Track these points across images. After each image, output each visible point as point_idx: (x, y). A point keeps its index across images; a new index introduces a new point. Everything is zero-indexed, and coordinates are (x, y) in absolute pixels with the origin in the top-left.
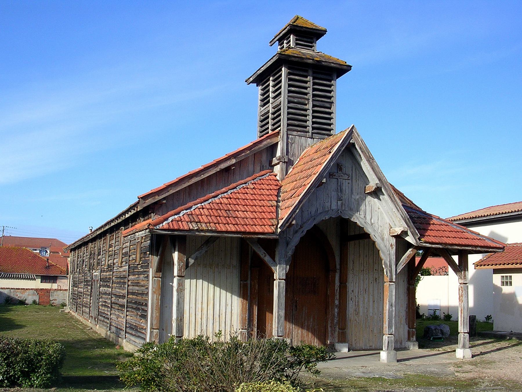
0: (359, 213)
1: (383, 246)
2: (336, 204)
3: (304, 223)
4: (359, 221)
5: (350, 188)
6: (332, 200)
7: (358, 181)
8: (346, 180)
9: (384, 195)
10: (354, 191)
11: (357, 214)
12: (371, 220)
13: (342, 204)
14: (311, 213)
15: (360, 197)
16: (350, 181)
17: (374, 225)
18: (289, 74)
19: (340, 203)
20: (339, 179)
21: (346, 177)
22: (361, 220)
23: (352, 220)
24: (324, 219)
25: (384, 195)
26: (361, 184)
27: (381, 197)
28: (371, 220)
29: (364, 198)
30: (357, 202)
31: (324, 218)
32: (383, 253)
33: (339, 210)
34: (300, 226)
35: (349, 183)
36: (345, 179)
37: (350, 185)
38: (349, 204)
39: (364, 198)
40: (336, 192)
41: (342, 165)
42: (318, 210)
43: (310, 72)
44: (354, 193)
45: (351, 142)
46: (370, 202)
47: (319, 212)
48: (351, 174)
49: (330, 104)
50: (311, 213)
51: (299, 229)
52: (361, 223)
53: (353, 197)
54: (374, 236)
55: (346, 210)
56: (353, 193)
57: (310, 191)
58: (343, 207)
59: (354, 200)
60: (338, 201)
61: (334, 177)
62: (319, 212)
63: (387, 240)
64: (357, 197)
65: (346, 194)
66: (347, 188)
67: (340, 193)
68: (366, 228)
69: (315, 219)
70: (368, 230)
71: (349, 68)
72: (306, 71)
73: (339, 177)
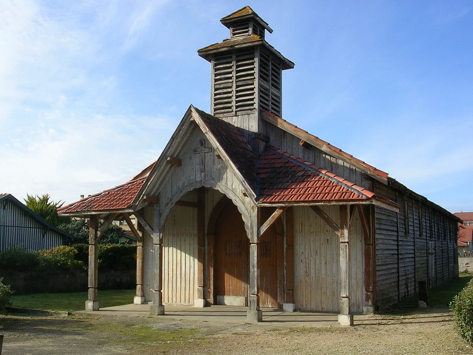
4: (220, 188)
8: (209, 153)
13: (205, 175)
17: (235, 190)
19: (203, 174)
20: (201, 154)
22: (222, 187)
24: (189, 190)
28: (232, 186)
30: (219, 171)
32: (245, 216)
33: (202, 181)
34: (170, 199)
35: (211, 155)
42: (184, 184)
43: (234, 57)
44: (216, 163)
47: (185, 185)
52: (222, 190)
53: (215, 167)
54: (235, 201)
59: (216, 170)
61: (197, 152)
62: (185, 185)
63: (248, 203)
64: (219, 167)
66: (209, 160)
70: (229, 196)
72: (231, 57)
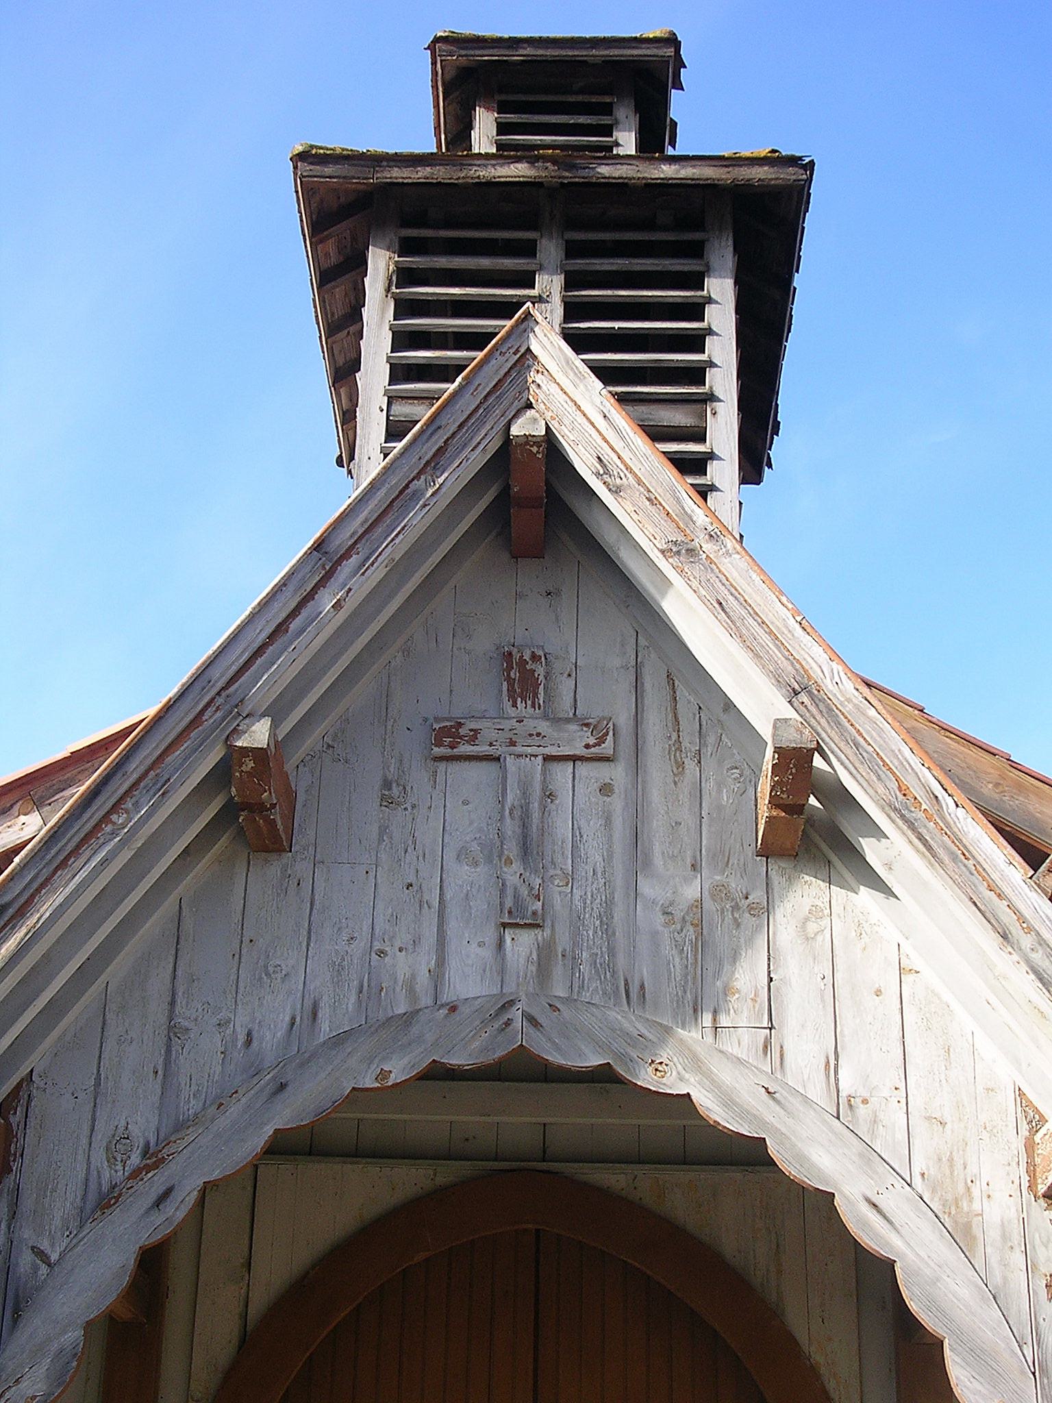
0: (707, 1019)
1: (965, 1292)
2: (487, 953)
3: (180, 1126)
4: (715, 1086)
5: (618, 822)
6: (453, 926)
7: (690, 765)
8: (583, 769)
9: (879, 833)
10: (657, 849)
11: (693, 1036)
12: (832, 1068)
13: (545, 957)
14: (249, 1041)
15: (719, 892)
16: (617, 773)
17: (862, 1110)
18: (405, 276)
19: (521, 945)
20: (510, 761)
21: (576, 741)
22: (726, 1075)
23: (646, 1079)
24: (369, 1082)
25: (879, 833)
26: (720, 785)
27: (871, 849)
28: (832, 1068)
29: (758, 896)
30: (690, 932)
31: (374, 1070)
32: (978, 1356)
33: (511, 1003)
34: (145, 1153)
35: (606, 789)
36: (574, 759)
37: (617, 803)
38: (612, 952)
39: (758, 896)
40: (489, 860)
41: (535, 657)
42: (315, 1015)
43: (550, 249)
44: (658, 861)
45: (515, 430)
46: (812, 927)
47: (325, 1028)
48: (624, 719)
49: (698, 406)
50: (249, 1041)
51: (136, 1174)
52: (728, 1101)
53: (647, 888)
54: (865, 1209)
55: (586, 996)
56: (648, 863)
57: (106, 818)
58: (559, 972)
59: (661, 919)
60: (508, 935)
61: (465, 749)
62: (325, 1028)
63: (1005, 1237)
64: (691, 891)
65: (585, 870)
66: (592, 828)
67: (517, 867)
68: (782, 1137)
69: (282, 1087)
70: (802, 1158)
71: (683, 89)
72: (529, 250)
73: (513, 743)
